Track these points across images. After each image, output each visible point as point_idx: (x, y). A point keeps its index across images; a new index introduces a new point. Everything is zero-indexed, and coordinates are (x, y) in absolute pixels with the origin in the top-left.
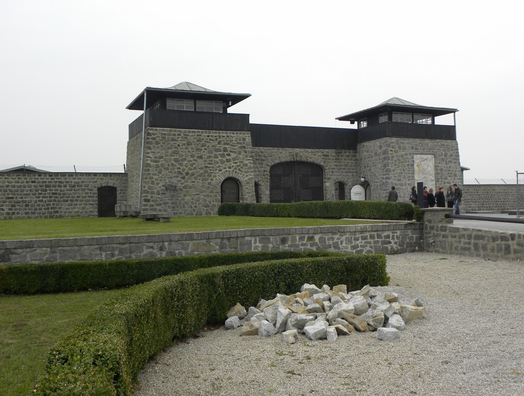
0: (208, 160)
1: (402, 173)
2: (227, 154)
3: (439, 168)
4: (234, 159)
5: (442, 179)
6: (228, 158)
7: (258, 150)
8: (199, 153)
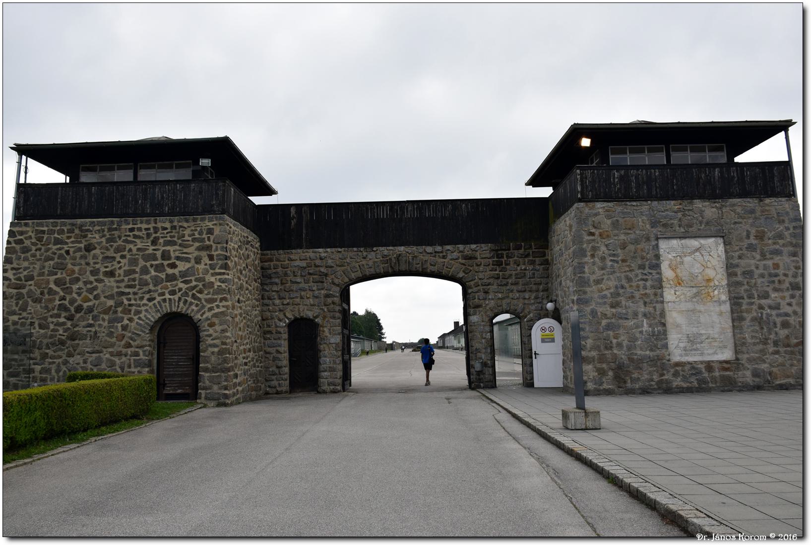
0: (126, 279)
1: (623, 287)
2: (168, 265)
3: (739, 271)
4: (183, 274)
5: (750, 297)
6: (170, 271)
7: (312, 255)
8: (109, 265)
